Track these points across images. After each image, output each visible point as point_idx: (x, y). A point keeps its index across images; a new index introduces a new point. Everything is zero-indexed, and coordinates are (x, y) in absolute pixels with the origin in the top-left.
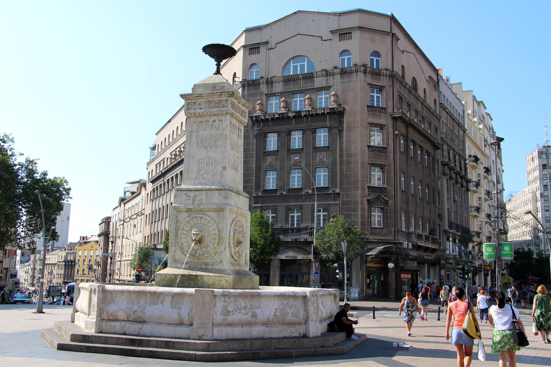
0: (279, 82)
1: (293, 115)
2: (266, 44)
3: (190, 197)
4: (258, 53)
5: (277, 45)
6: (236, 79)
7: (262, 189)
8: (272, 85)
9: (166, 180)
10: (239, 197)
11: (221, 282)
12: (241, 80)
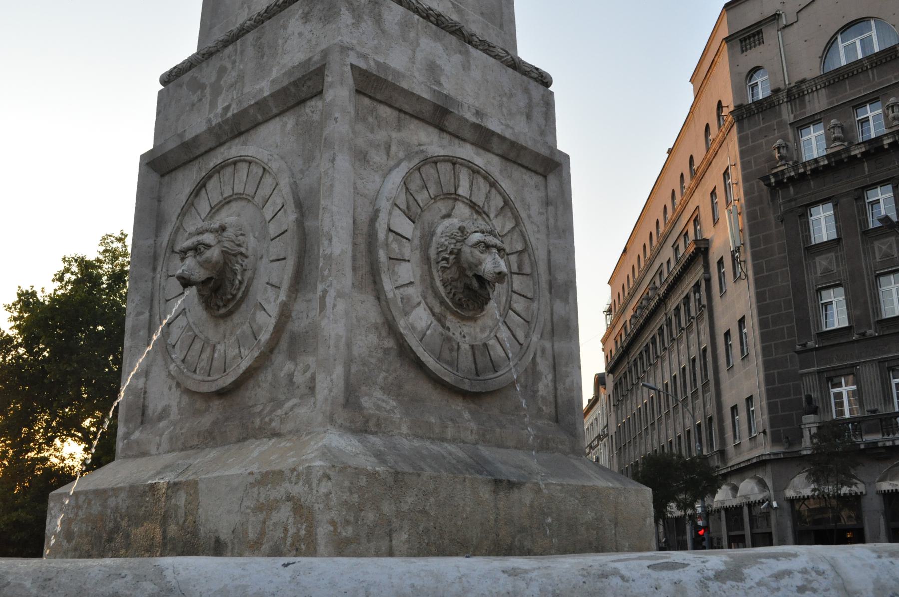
0: (817, 90)
1: (863, 150)
2: (774, 20)
3: (202, 87)
4: (759, 44)
5: (799, 14)
6: (725, 112)
7: (813, 333)
8: (802, 102)
9: (632, 363)
10: (467, 53)
11: (275, 517)
12: (732, 108)
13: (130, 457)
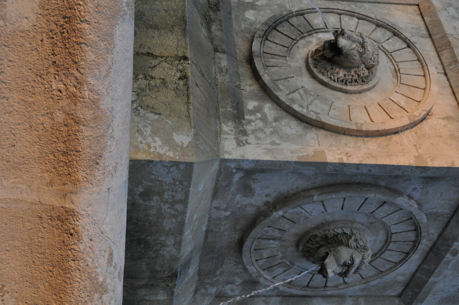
13: (218, 176)
